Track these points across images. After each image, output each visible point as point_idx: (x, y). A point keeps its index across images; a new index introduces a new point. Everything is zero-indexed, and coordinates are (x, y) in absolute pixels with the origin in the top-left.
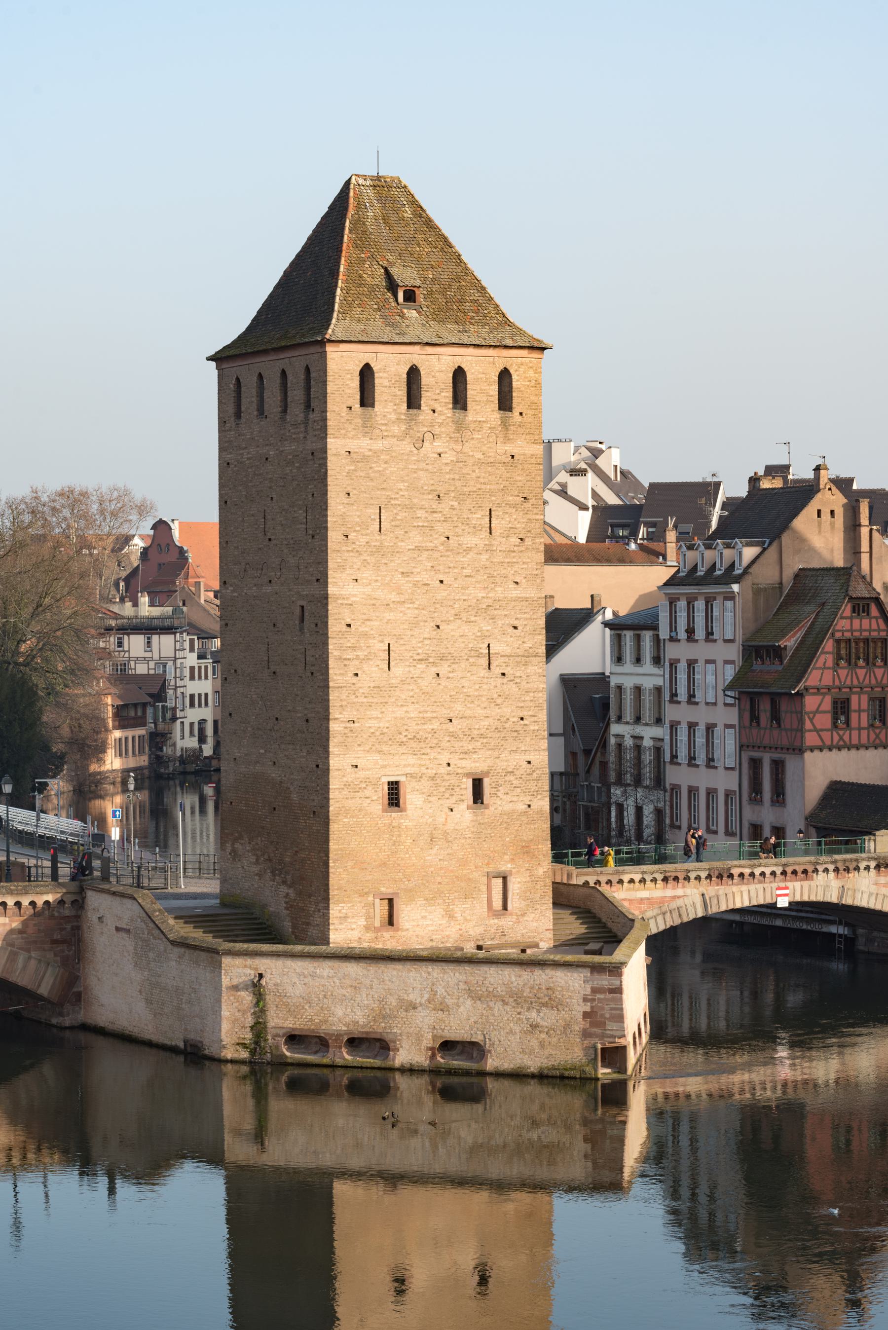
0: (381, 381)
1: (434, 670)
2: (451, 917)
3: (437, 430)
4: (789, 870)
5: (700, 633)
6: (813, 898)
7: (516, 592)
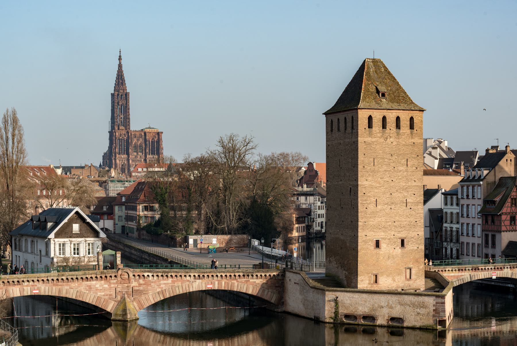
1: (390, 207)
2: (394, 281)
3: (391, 135)
4: (496, 267)
5: (470, 196)
6: (503, 276)
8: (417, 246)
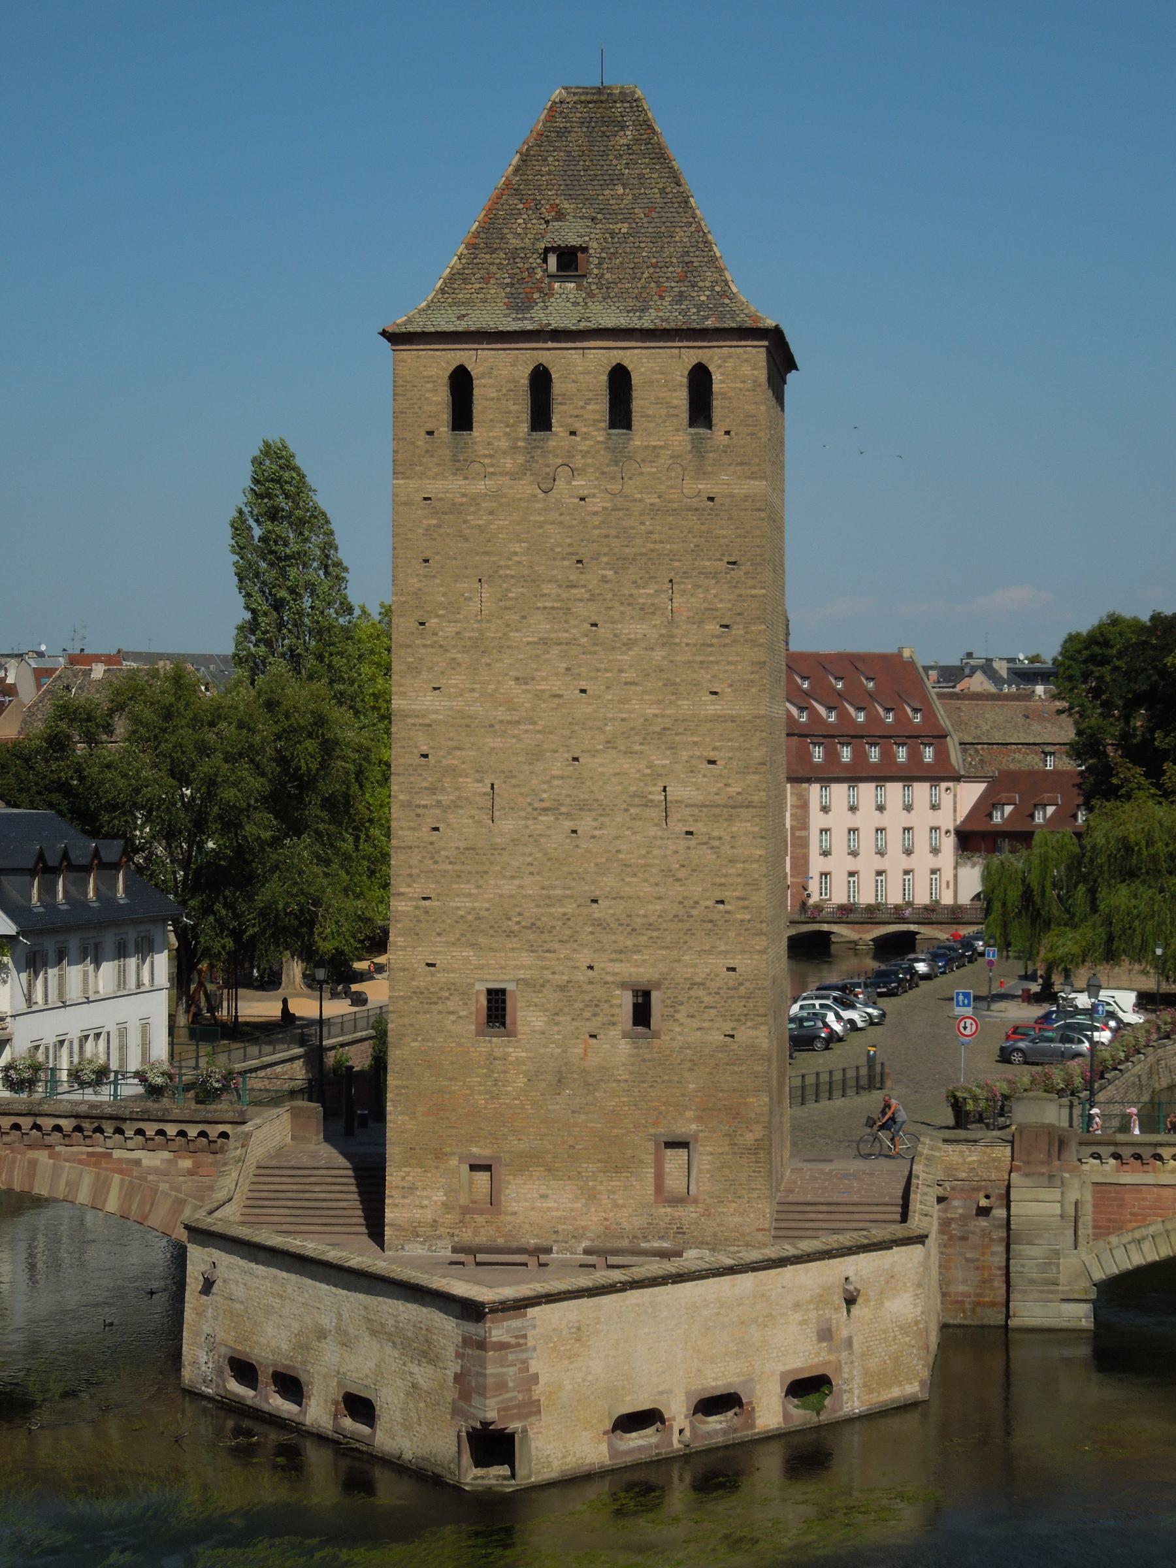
0: (482, 393)
1: (568, 825)
3: (578, 462)
7: (713, 708)
8: (727, 1027)
